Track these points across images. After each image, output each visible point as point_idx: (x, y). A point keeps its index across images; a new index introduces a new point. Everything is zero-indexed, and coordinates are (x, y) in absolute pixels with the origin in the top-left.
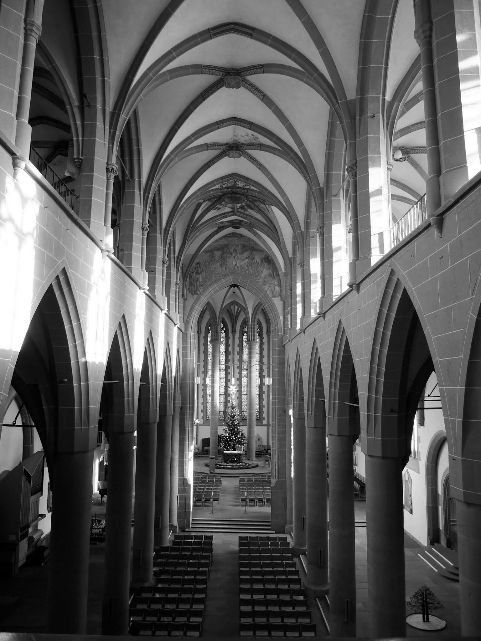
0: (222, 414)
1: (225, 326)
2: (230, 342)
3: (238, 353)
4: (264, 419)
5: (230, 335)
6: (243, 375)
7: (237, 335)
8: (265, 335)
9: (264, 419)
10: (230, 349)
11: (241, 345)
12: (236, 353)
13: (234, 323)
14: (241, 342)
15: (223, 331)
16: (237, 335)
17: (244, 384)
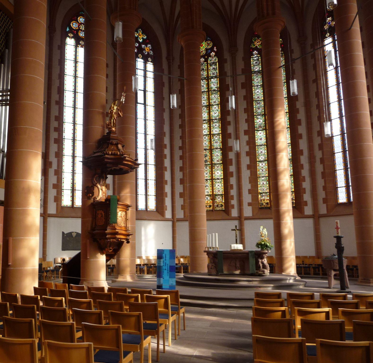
0: (219, 200)
1: (216, 42)
2: (228, 67)
3: (244, 86)
4: (306, 204)
5: (227, 56)
6: (257, 125)
7: (240, 54)
8: (295, 46)
9: (306, 204)
10: (229, 81)
11: (248, 72)
12: (239, 86)
13: (231, 27)
14: (248, 65)
15: (213, 54)
16: (240, 54)
17: (258, 142)
